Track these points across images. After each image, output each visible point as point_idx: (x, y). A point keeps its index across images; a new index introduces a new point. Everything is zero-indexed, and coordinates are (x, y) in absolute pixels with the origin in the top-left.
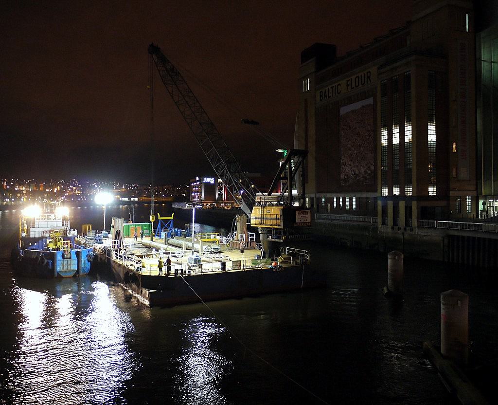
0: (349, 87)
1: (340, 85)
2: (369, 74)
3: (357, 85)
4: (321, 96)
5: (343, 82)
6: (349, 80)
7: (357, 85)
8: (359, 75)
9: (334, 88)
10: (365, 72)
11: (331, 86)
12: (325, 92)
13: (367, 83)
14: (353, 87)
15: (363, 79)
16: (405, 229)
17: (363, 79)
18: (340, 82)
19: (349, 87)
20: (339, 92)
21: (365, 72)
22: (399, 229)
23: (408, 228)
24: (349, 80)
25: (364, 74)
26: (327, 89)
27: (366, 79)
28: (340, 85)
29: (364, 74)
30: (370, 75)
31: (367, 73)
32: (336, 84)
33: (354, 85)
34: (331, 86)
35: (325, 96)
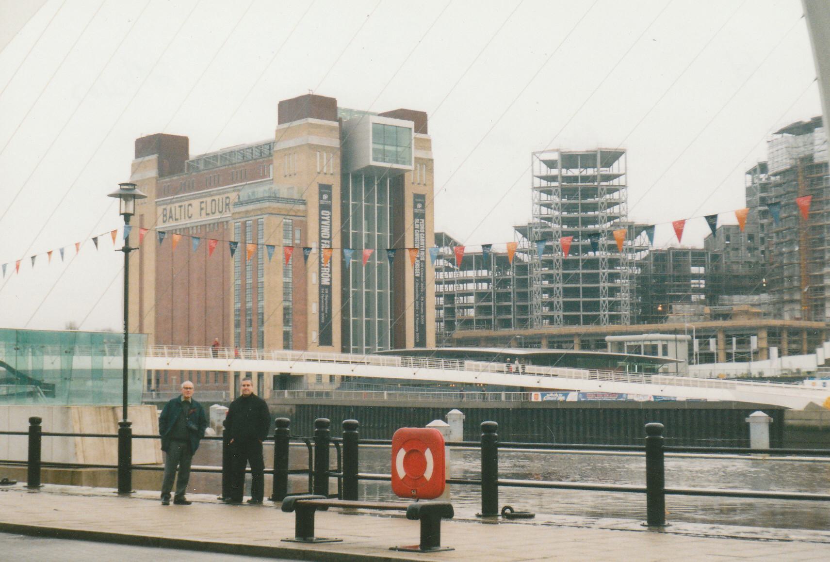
0: (203, 212)
1: (190, 205)
3: (213, 211)
4: (165, 216)
5: (196, 203)
6: (202, 202)
8: (216, 198)
9: (183, 208)
11: (180, 204)
12: (171, 211)
15: (221, 204)
17: (221, 204)
18: (192, 202)
19: (203, 212)
25: (222, 199)
26: (173, 206)
27: (224, 206)
28: (190, 205)
29: (222, 199)
32: (187, 203)
33: (209, 211)
35: (171, 217)
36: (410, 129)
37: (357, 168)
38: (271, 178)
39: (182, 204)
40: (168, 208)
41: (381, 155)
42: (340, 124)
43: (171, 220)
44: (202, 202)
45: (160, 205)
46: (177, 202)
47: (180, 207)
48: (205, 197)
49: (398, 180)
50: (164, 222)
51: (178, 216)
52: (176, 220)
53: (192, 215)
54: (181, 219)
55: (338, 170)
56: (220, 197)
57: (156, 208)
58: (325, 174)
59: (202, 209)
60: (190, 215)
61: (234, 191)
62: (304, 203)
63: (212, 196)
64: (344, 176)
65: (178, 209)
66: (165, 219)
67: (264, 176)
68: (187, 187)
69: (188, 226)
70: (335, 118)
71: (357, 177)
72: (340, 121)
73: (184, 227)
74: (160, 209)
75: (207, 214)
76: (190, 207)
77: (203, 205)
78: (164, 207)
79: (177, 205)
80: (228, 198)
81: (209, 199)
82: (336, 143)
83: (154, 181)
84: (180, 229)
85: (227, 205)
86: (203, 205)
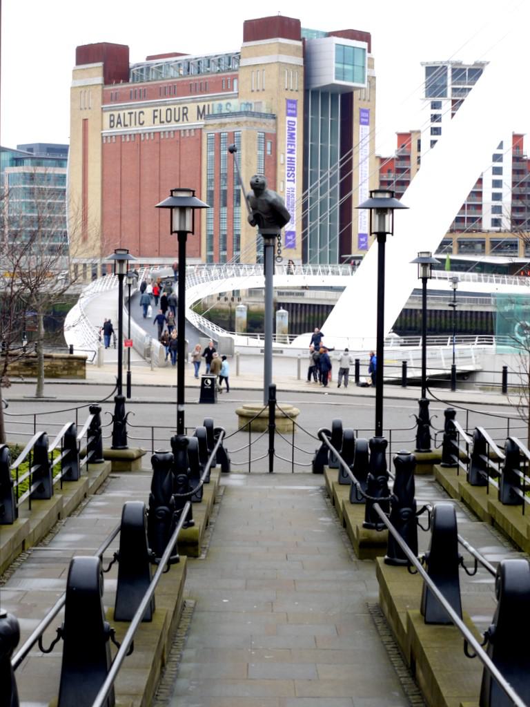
0: (157, 120)
1: (142, 112)
2: (185, 110)
4: (111, 121)
5: (148, 112)
6: (157, 110)
7: (169, 119)
8: (172, 107)
9: (133, 116)
10: (181, 106)
13: (183, 120)
14: (162, 120)
16: (233, 299)
19: (157, 120)
20: (141, 122)
21: (181, 106)
22: (226, 299)
23: (236, 299)
24: (157, 110)
25: (179, 108)
26: (121, 113)
28: (142, 112)
29: (179, 108)
30: (187, 113)
31: (184, 108)
32: (138, 111)
33: (163, 119)
34: (130, 111)
35: (119, 123)
36: (364, 49)
37: (317, 85)
38: (235, 91)
39: (133, 111)
40: (116, 114)
41: (341, 74)
42: (304, 44)
43: (119, 125)
44: (155, 111)
45: (106, 111)
46: (127, 109)
47: (130, 113)
48: (160, 105)
49: (347, 98)
50: (111, 127)
51: (127, 122)
52: (125, 126)
53: (143, 122)
54: (131, 125)
55: (301, 87)
56: (177, 107)
57: (102, 115)
58: (292, 90)
59: (155, 117)
60: (141, 122)
61: (193, 102)
62: (274, 117)
63: (166, 105)
64: (306, 91)
65: (127, 116)
66: (112, 124)
67: (227, 90)
68: (135, 95)
69: (140, 132)
70: (300, 40)
71: (315, 93)
72: (303, 40)
73: (135, 132)
74: (107, 116)
75: (161, 122)
76: (141, 114)
77: (156, 114)
78: (112, 113)
79: (126, 112)
80: (186, 108)
81: (164, 109)
82: (299, 61)
83: (100, 87)
84: (130, 135)
85: (184, 114)
86: (156, 114)
